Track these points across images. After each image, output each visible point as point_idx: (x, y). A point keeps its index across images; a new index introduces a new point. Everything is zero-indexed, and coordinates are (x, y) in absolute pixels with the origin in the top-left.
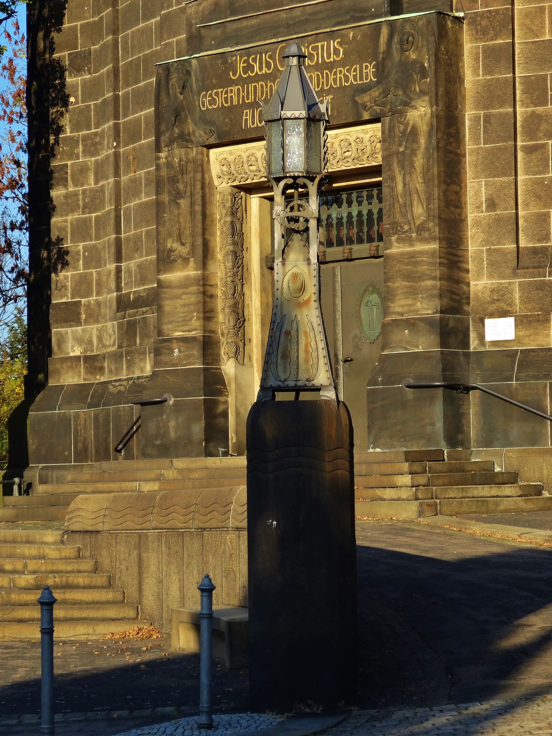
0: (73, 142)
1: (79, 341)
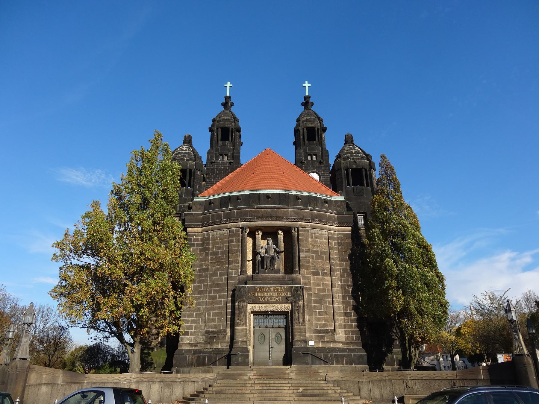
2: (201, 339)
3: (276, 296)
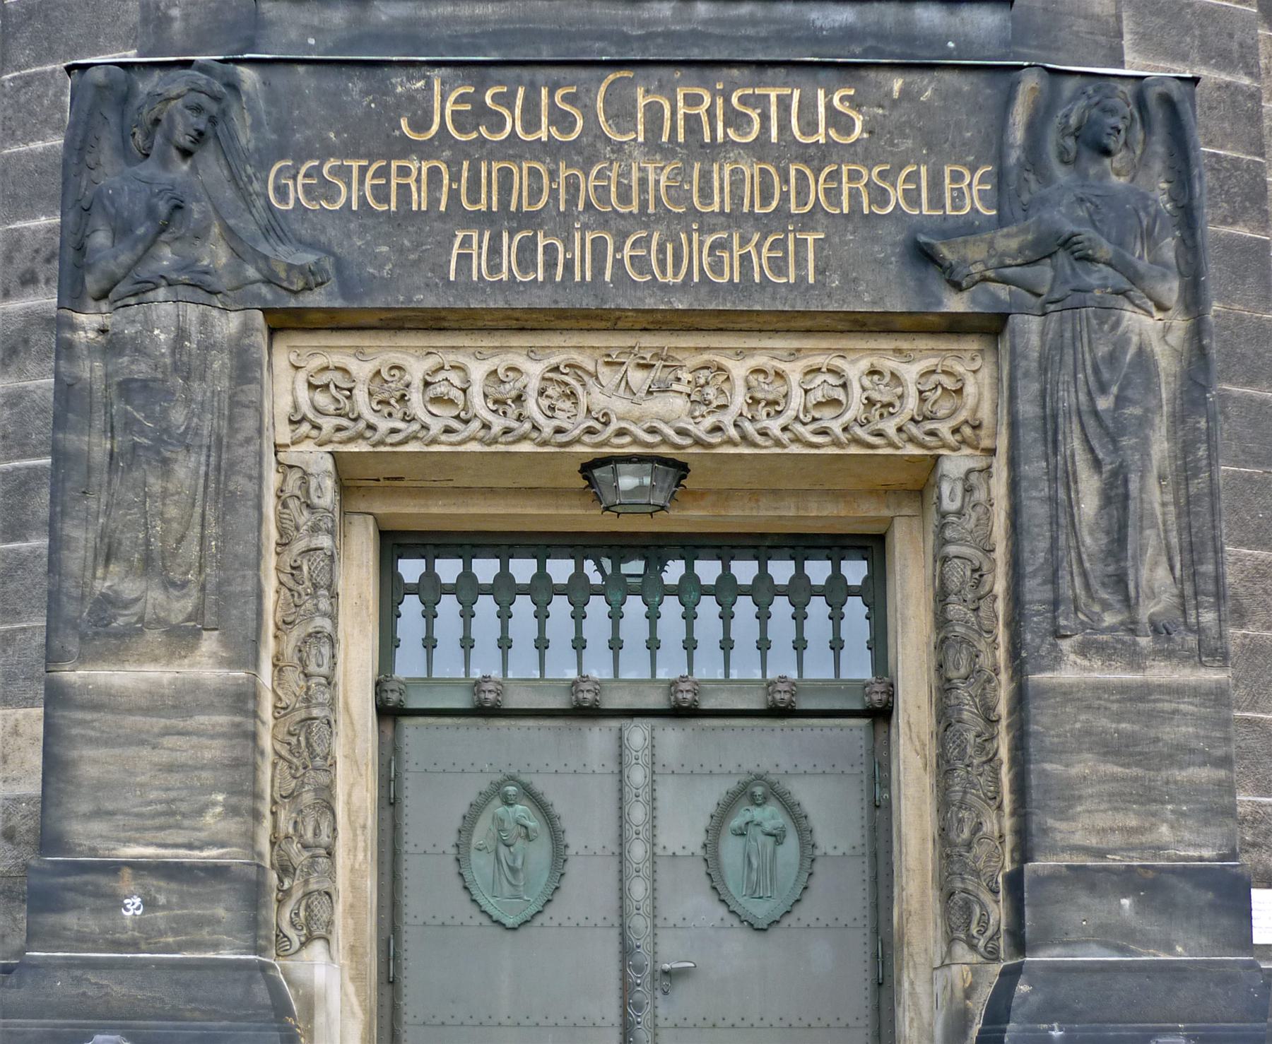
3: (734, 218)
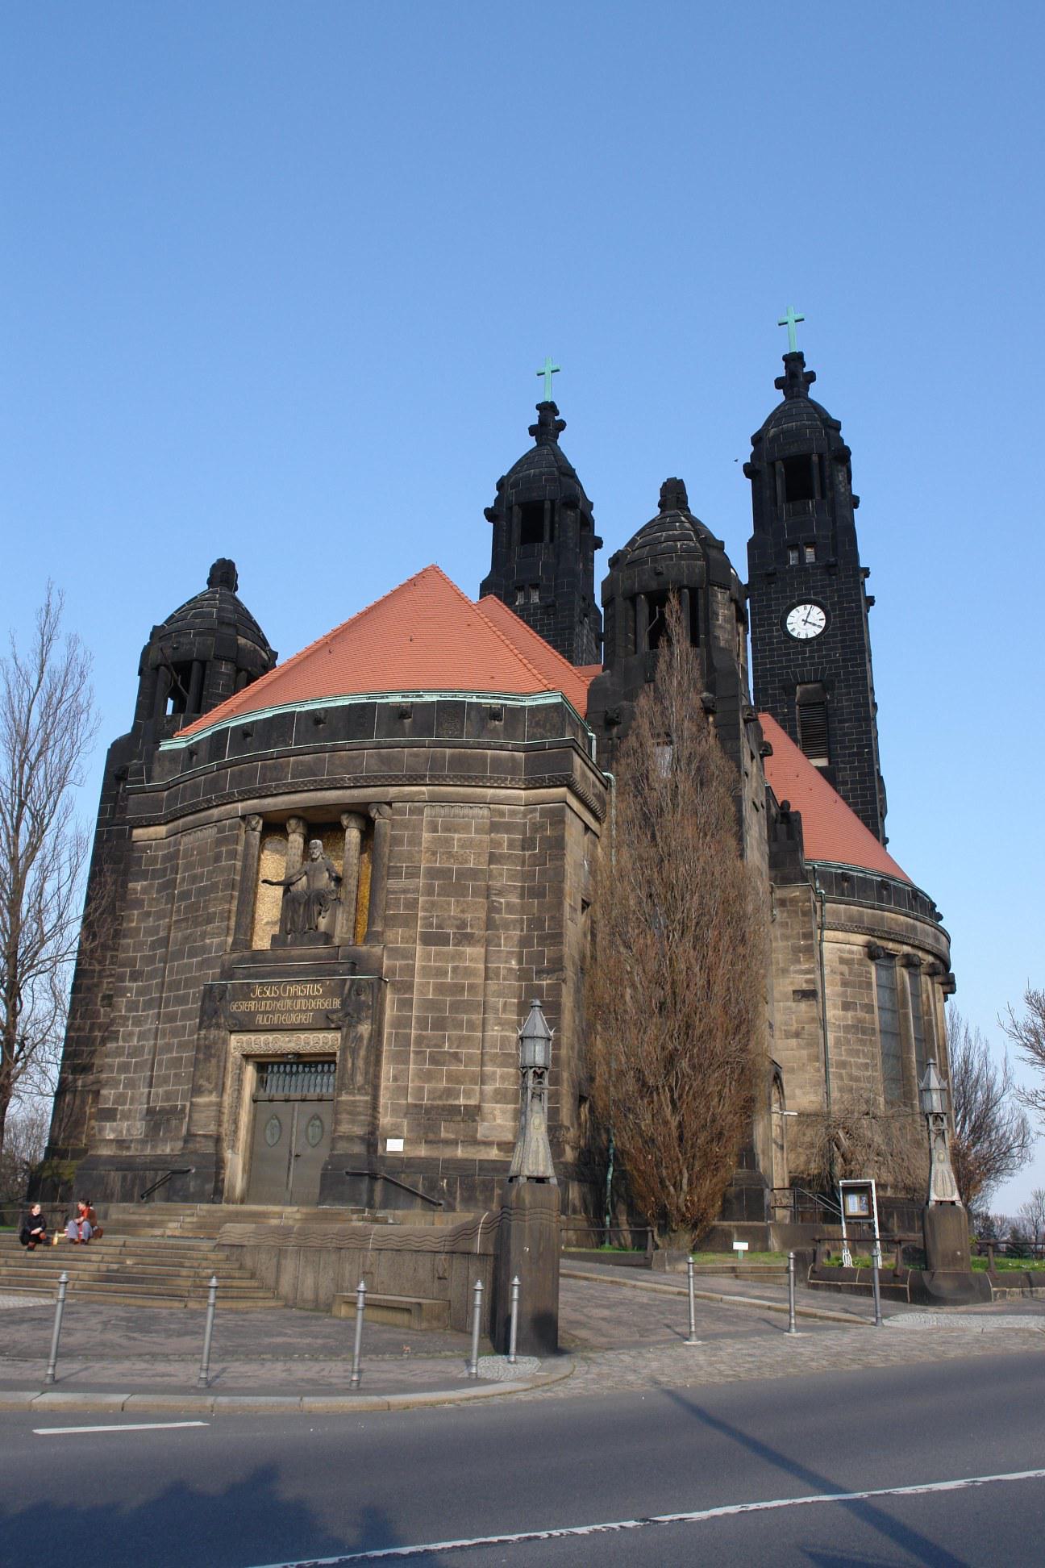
0: (126, 1018)
1: (113, 1130)
2: (139, 1128)
3: (301, 1011)
